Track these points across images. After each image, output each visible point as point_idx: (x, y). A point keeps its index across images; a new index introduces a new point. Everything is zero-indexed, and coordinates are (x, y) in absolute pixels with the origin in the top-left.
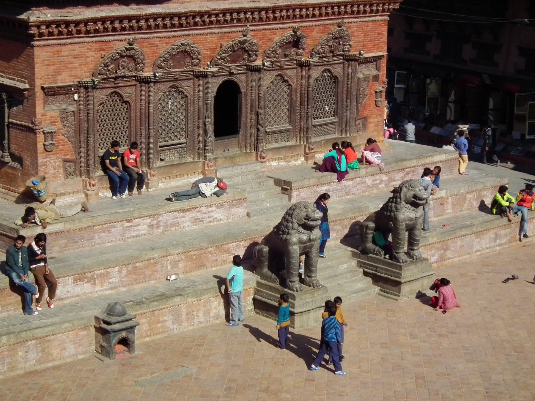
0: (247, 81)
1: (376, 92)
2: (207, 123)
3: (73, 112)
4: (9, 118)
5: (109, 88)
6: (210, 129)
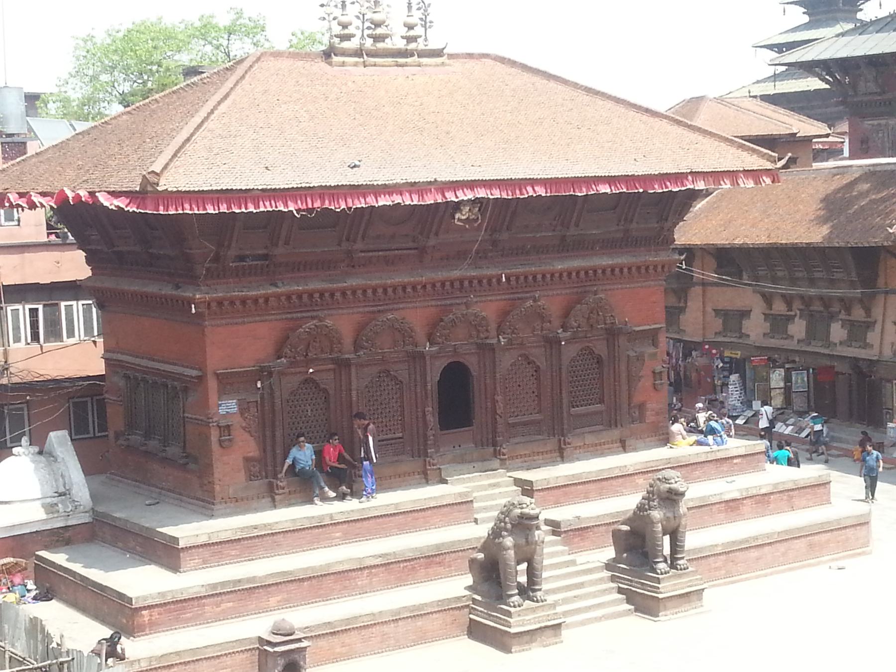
0: (479, 363)
1: (654, 372)
2: (427, 413)
3: (257, 402)
4: (184, 412)
5: (296, 373)
6: (432, 419)
